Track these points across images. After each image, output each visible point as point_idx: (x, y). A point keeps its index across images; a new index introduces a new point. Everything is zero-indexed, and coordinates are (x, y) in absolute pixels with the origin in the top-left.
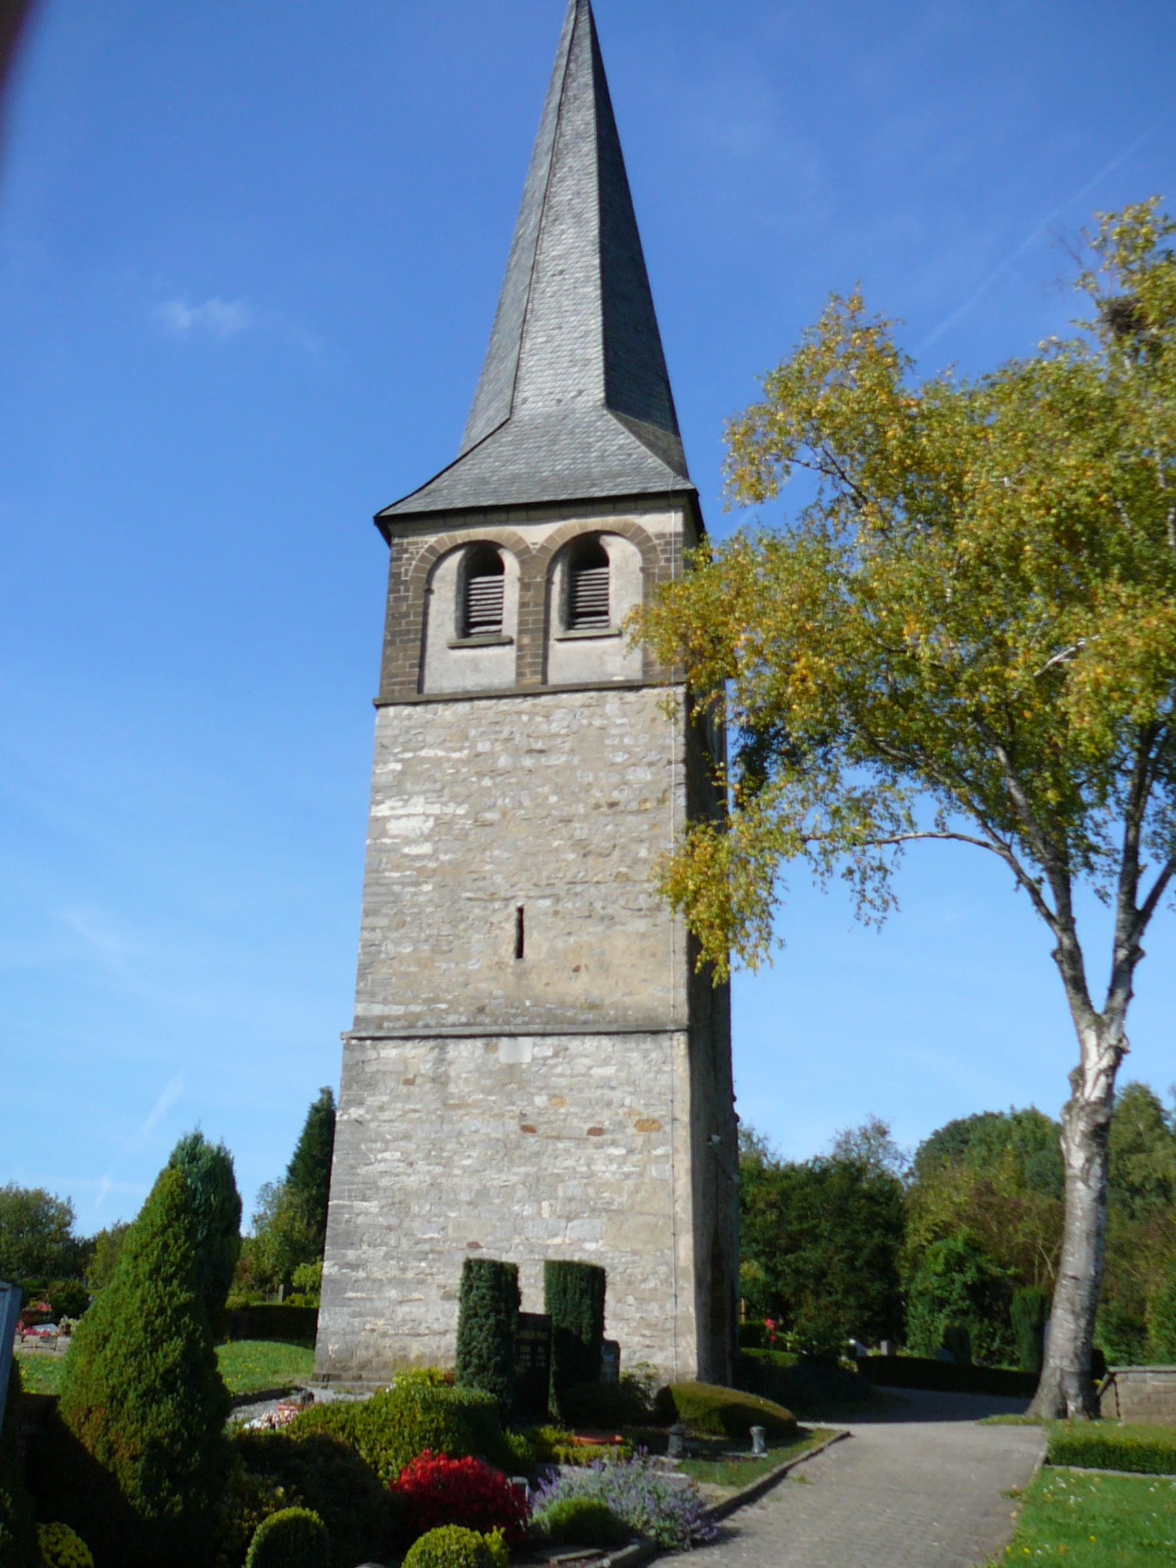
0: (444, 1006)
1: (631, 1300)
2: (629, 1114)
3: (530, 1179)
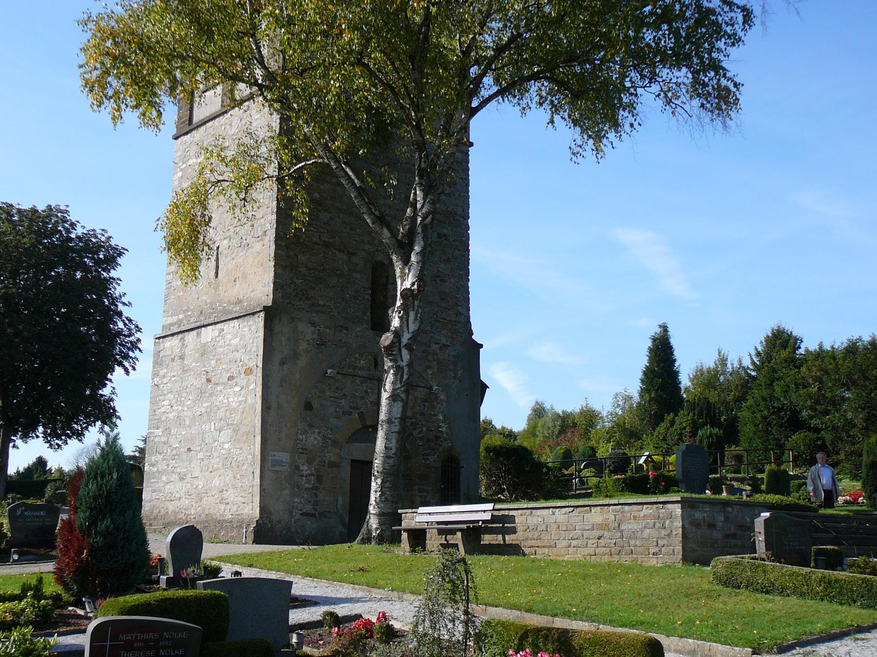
2: (242, 366)
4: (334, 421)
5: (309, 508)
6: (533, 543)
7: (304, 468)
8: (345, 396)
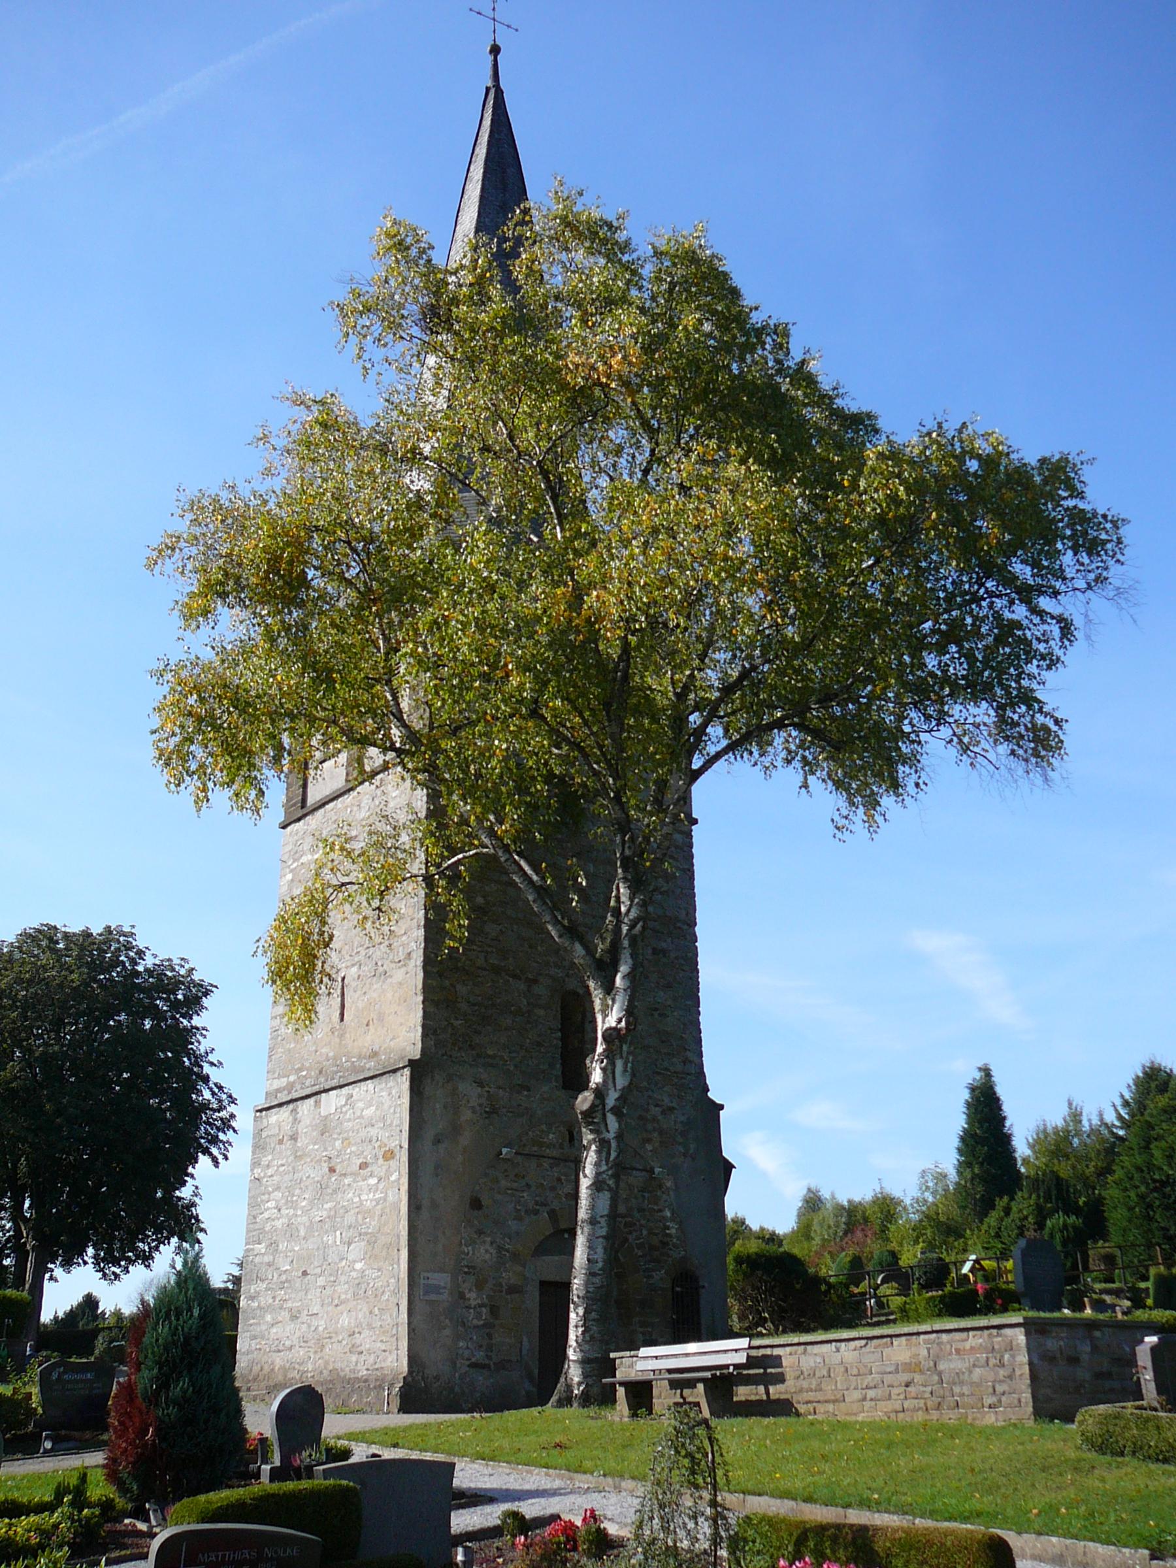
0: (304, 1073)
1: (376, 1311)
2: (380, 1147)
3: (332, 1213)
4: (513, 1225)
5: (479, 1356)
6: (811, 1396)
7: (472, 1295)
8: (527, 1185)
